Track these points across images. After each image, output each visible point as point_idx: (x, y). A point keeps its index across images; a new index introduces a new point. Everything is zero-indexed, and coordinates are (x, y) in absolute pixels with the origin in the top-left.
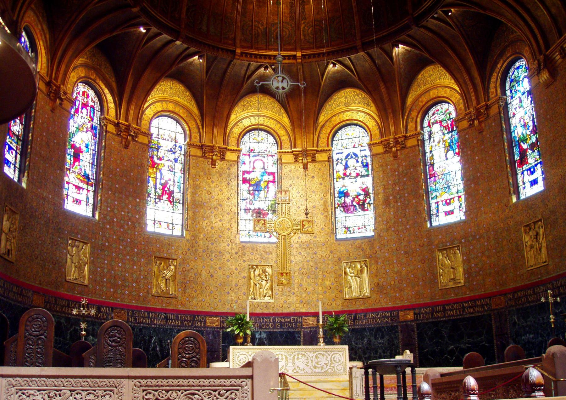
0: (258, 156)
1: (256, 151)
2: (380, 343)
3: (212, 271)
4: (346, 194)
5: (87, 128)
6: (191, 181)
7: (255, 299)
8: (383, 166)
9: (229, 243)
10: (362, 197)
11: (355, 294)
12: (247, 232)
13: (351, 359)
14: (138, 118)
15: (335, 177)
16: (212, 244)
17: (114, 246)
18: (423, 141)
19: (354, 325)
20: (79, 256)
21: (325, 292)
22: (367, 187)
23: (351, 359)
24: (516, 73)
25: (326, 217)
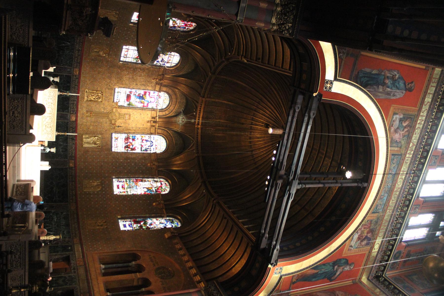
1: (159, 99)
2: (59, 150)
4: (133, 140)
5: (175, 25)
7: (86, 92)
9: (115, 83)
10: (131, 147)
11: (84, 140)
13: (49, 142)
18: (154, 178)
19: (70, 139)
21: (86, 125)
22: (136, 150)
23: (49, 142)
24: (176, 222)
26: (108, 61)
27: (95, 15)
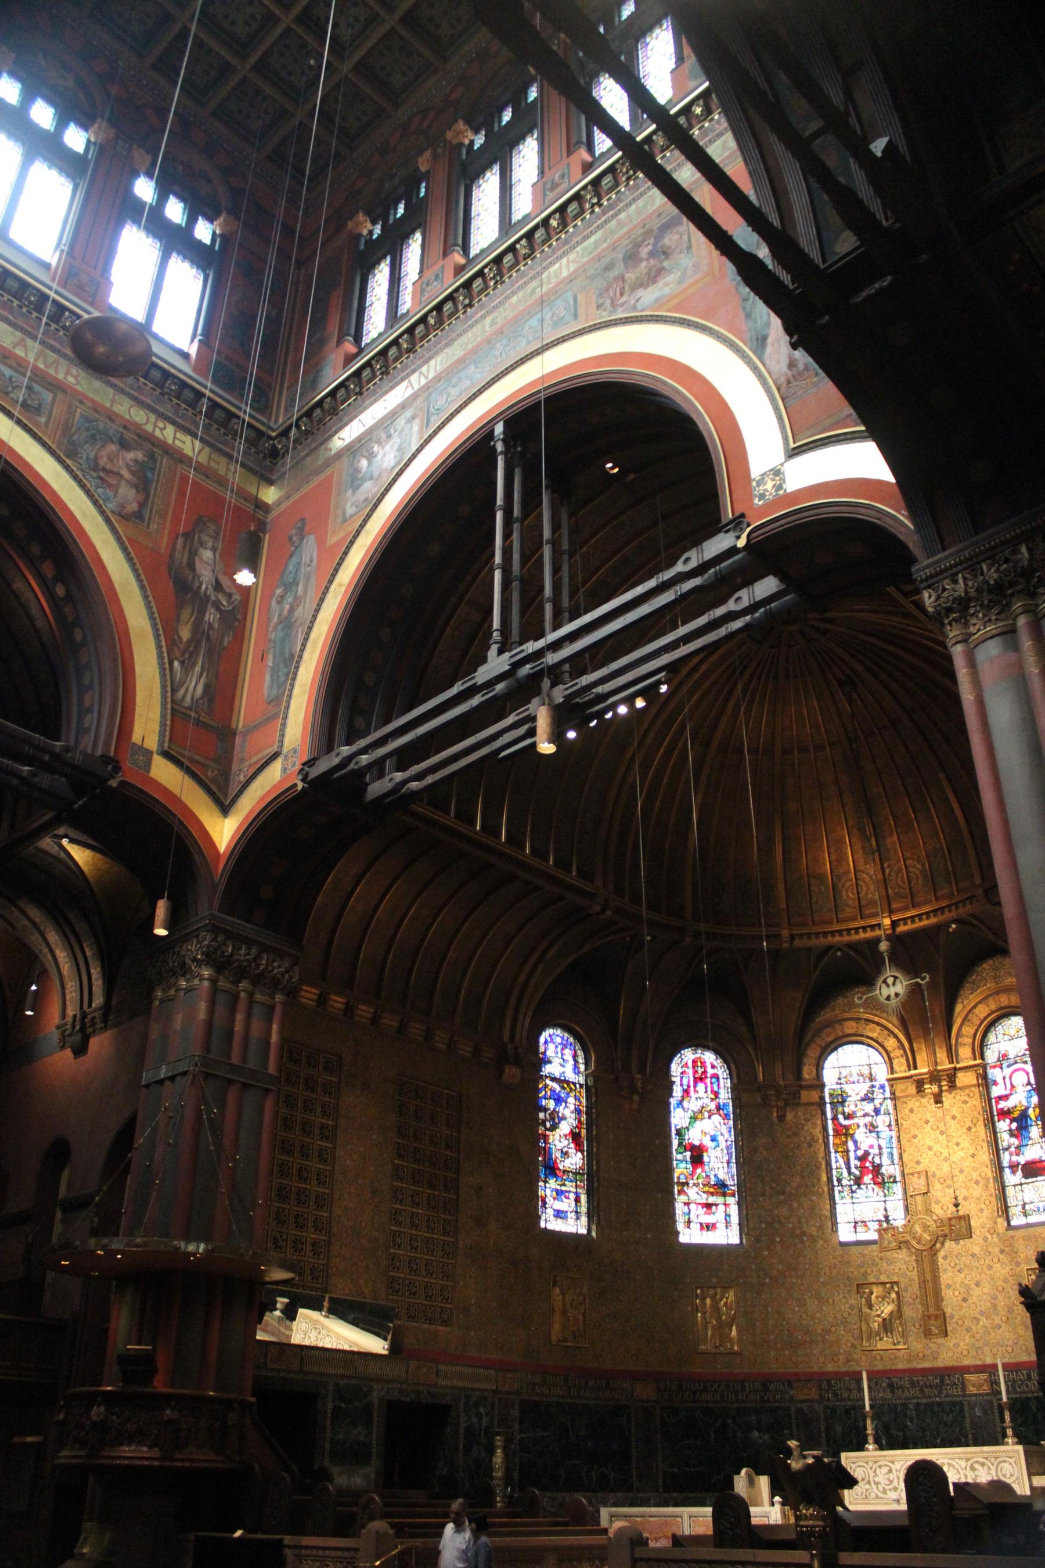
0: (1016, 1062)
1: (1011, 1056)
5: (710, 1111)
12: (1020, 1208)
20: (718, 1310)
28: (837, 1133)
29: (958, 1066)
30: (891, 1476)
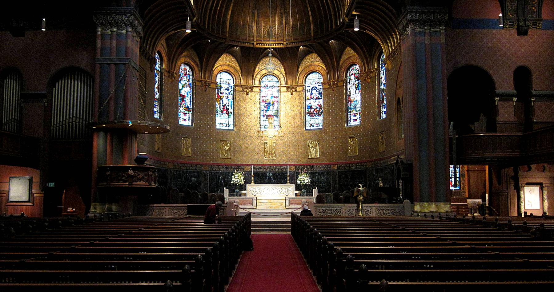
3: (247, 145)
4: (311, 107)
6: (236, 104)
8: (328, 95)
11: (312, 157)
14: (210, 76)
15: (306, 99)
16: (247, 133)
17: (202, 137)
18: (347, 83)
25: (301, 119)
26: (234, 141)
27: (134, 168)
28: (218, 98)
29: (254, 86)
30: (260, 190)
